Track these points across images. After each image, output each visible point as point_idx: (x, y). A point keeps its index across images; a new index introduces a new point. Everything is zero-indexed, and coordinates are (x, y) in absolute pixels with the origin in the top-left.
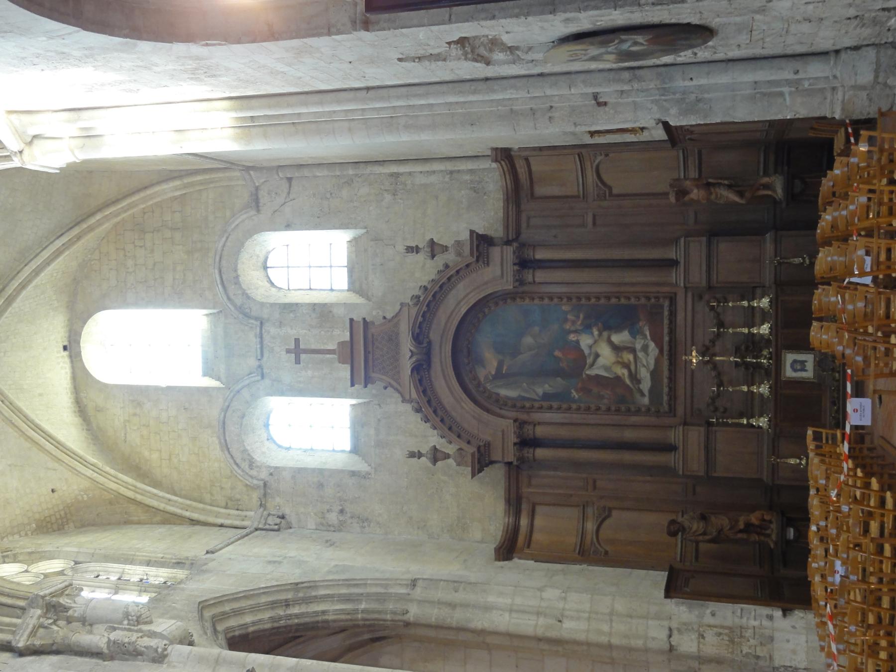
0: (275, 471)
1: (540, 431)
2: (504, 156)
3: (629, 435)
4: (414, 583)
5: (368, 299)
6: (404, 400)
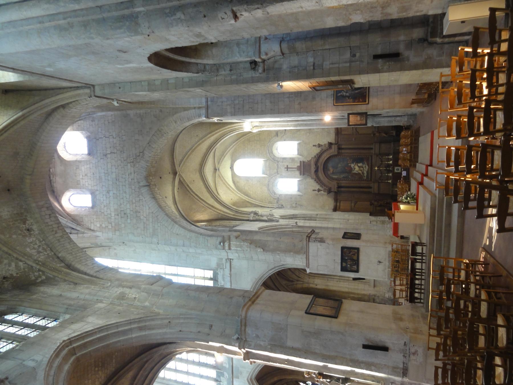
0: (280, 195)
1: (342, 185)
3: (362, 185)
4: (317, 215)
6: (312, 178)
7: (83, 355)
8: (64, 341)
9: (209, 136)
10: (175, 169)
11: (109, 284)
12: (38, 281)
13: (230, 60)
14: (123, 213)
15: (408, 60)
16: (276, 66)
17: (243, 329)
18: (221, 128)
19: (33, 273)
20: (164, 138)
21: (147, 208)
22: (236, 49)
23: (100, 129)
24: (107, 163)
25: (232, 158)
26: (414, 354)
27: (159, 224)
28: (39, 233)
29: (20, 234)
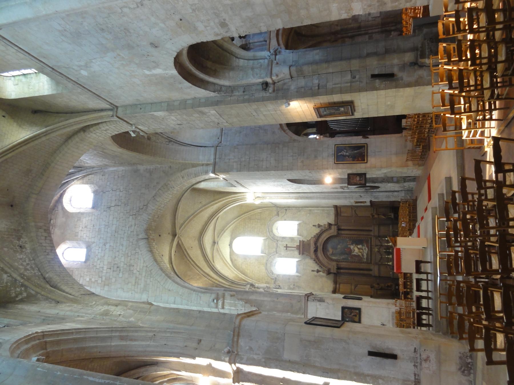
0: (278, 275)
1: (342, 266)
2: (336, 207)
5: (302, 236)
6: (311, 258)
7: (54, 352)
8: (36, 333)
9: (212, 203)
10: (175, 231)
11: (94, 303)
12: (17, 299)
13: (244, 82)
14: (116, 266)
15: (402, 80)
16: (285, 87)
17: (235, 340)
18: (224, 197)
19: (15, 288)
20: (169, 192)
21: (142, 261)
22: (250, 72)
23: (108, 183)
24: (110, 215)
25: (231, 236)
26: (426, 360)
27: (152, 279)
28: (31, 253)
29: (11, 249)
